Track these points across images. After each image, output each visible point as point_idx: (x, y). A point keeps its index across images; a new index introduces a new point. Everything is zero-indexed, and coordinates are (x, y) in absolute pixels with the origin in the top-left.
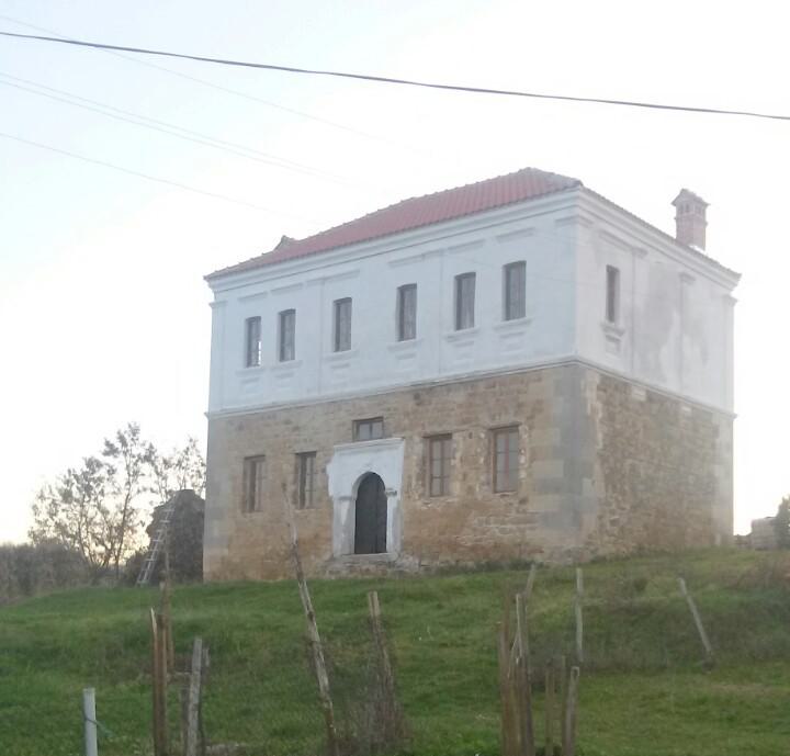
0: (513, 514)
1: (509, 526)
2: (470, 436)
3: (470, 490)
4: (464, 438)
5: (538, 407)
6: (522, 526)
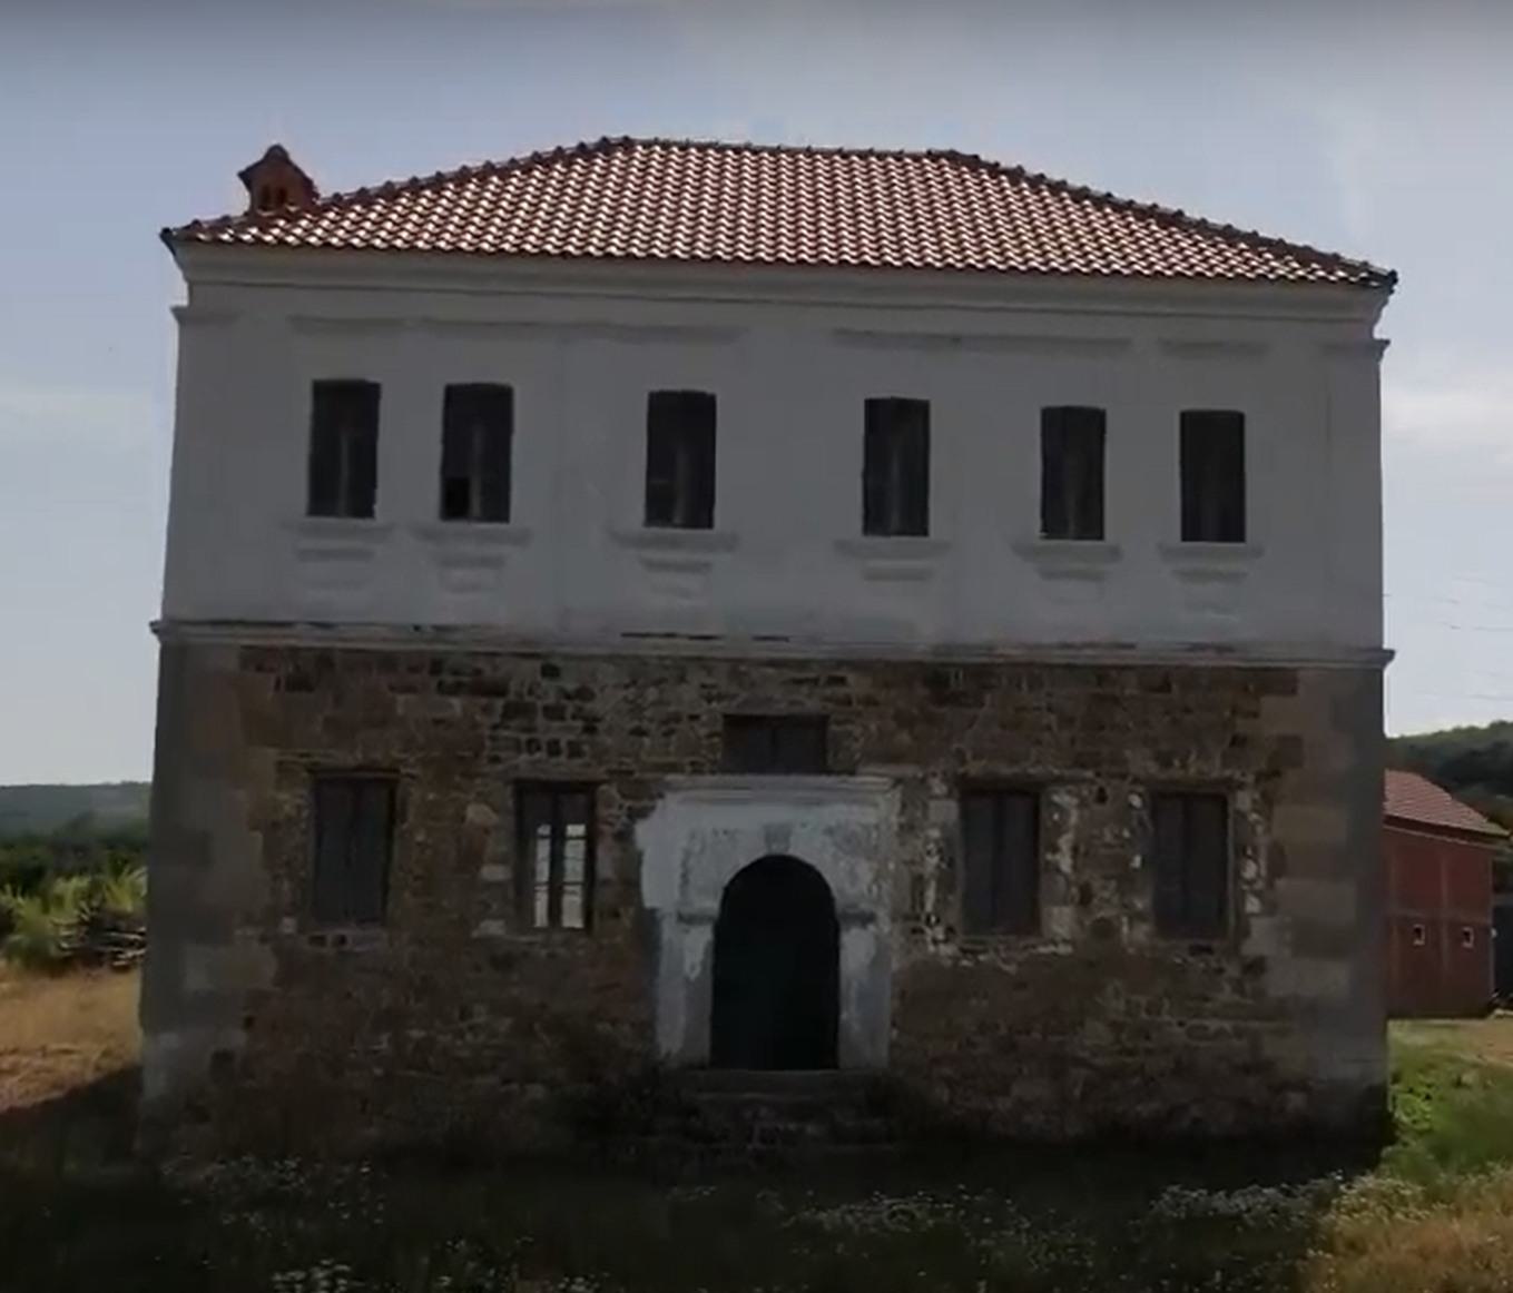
0: (1226, 994)
1: (1213, 1025)
2: (1102, 797)
3: (1105, 930)
4: (1083, 804)
5: (1287, 753)
6: (1255, 1025)
